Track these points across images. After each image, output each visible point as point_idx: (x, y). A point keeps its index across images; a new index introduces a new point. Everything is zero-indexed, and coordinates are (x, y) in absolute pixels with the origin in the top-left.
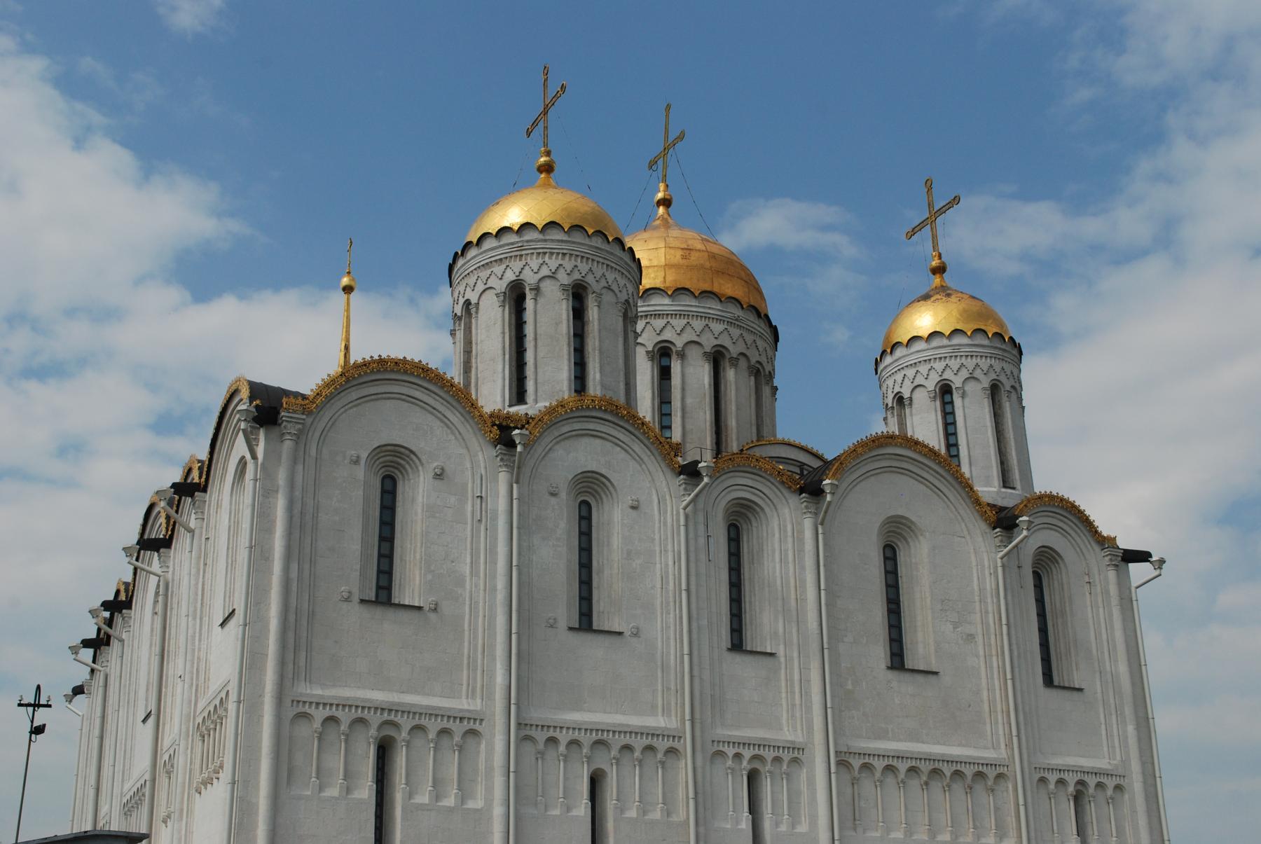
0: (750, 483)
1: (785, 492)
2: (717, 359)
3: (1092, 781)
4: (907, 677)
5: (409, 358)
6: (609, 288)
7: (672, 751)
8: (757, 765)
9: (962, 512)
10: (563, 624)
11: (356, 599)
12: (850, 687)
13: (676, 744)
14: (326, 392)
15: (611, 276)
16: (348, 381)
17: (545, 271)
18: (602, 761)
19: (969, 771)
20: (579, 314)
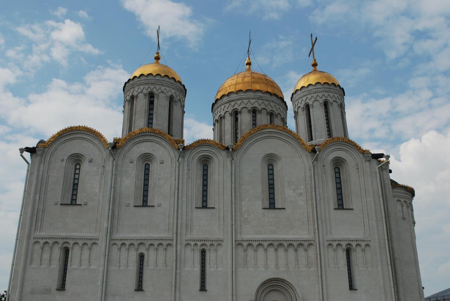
0: (207, 149)
1: (220, 151)
2: (254, 111)
3: (354, 244)
4: (277, 211)
5: (81, 125)
6: (162, 92)
7: (169, 245)
8: (204, 247)
9: (298, 149)
10: (332, 207)
11: (132, 205)
12: (246, 217)
13: (171, 242)
14: (52, 140)
15: (163, 88)
16: (59, 136)
17: (140, 91)
18: (142, 250)
19: (295, 244)
20: (151, 103)
